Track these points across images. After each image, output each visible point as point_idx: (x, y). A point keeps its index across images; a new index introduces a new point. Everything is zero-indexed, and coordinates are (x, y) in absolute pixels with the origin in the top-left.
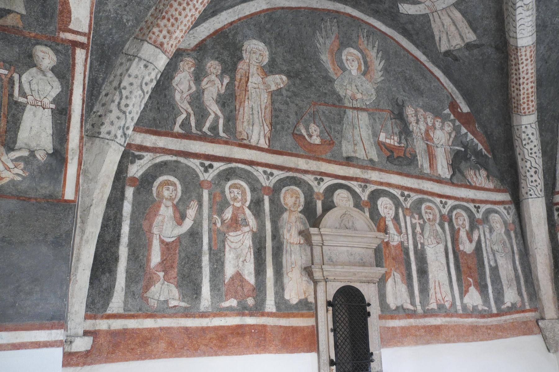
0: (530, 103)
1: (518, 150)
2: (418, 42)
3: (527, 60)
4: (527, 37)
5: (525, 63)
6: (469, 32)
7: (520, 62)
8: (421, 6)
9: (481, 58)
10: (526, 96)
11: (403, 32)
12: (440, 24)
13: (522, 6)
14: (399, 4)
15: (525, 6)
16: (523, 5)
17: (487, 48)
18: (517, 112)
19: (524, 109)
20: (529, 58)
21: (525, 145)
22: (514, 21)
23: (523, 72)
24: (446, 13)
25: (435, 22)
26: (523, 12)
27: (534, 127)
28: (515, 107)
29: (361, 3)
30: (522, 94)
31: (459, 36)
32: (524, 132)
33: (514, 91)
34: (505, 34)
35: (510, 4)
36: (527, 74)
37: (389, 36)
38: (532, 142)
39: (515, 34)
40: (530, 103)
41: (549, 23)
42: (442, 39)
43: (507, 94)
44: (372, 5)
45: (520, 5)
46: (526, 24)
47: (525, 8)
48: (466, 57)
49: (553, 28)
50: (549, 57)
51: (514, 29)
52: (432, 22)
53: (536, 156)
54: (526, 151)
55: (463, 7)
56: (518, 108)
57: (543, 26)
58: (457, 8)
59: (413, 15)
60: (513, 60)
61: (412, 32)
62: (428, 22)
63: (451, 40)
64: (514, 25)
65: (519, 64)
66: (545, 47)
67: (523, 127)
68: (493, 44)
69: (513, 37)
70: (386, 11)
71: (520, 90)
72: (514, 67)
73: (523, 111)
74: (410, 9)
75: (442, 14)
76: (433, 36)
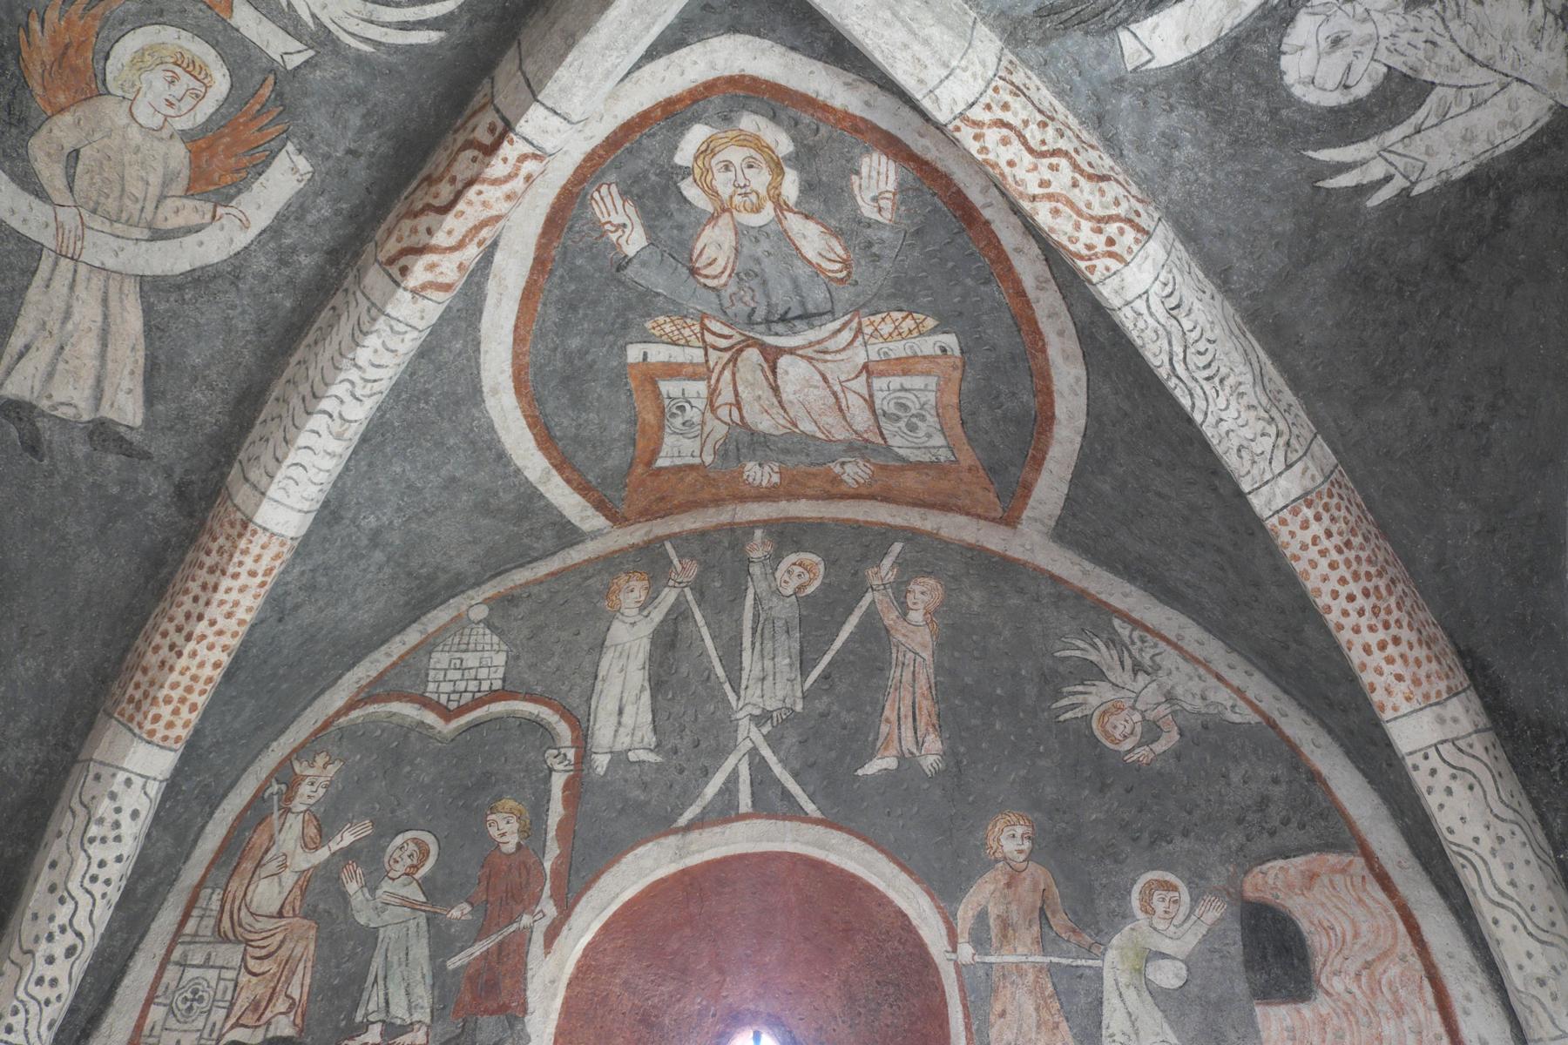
0: (185, 709)
1: (56, 849)
3: (253, 574)
4: (292, 508)
5: (244, 579)
6: (130, 391)
7: (231, 570)
8: (41, 211)
9: (115, 490)
10: (185, 681)
12: (59, 304)
13: (331, 416)
15: (338, 421)
16: (335, 415)
17: (154, 474)
18: (131, 719)
19: (156, 718)
20: (260, 572)
21: (92, 840)
23: (222, 603)
24: (101, 284)
25: (48, 286)
27: (152, 793)
28: (131, 700)
30: (178, 668)
31: (91, 381)
32: (113, 796)
33: (157, 649)
34: (230, 464)
35: (305, 389)
36: (229, 615)
38: (118, 839)
39: (265, 479)
40: (185, 709)
41: (350, 515)
42: (32, 353)
43: (126, 650)
45: (330, 410)
46: (312, 471)
47: (336, 426)
48: (71, 459)
49: (350, 535)
50: (297, 607)
51: (271, 464)
52: (38, 280)
53: (104, 895)
54: (82, 862)
55: (162, 307)
56: (138, 708)
57: (332, 513)
58: (143, 295)
60: (214, 553)
62: (23, 272)
63: (57, 376)
64: (279, 454)
65: (224, 573)
66: (303, 573)
67: (121, 776)
69: (255, 487)
71: (180, 654)
72: (202, 575)
73: (148, 726)
75: (89, 280)
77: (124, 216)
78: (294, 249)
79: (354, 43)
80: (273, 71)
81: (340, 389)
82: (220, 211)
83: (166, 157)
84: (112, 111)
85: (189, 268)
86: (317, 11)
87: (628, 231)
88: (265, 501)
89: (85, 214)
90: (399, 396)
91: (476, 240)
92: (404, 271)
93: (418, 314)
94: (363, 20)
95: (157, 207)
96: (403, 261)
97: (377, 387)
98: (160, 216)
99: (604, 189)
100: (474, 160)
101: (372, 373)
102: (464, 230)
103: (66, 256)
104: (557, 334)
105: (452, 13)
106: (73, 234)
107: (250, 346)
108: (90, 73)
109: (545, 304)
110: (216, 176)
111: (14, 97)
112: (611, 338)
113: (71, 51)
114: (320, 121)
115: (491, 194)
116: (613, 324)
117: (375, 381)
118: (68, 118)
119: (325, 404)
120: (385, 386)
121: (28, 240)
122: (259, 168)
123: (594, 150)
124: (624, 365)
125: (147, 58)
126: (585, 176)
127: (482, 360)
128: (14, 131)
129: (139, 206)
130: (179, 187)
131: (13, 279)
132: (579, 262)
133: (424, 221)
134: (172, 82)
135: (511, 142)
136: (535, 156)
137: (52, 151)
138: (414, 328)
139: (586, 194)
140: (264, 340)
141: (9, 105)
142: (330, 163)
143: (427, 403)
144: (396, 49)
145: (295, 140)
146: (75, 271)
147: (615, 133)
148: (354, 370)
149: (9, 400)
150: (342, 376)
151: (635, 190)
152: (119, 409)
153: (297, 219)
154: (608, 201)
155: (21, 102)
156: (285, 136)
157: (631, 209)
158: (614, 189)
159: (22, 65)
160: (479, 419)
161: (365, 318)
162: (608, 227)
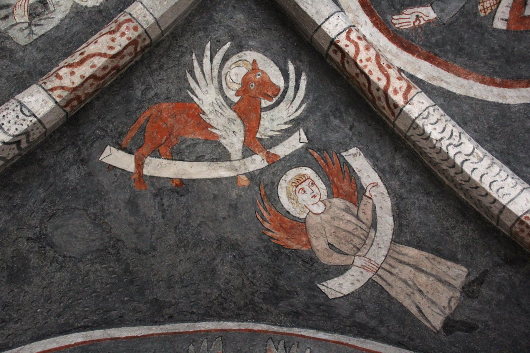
2: (392, 336)
4: (519, 194)
8: (353, 271)
9: (502, 297)
11: (358, 332)
12: (399, 283)
13: (466, 160)
14: (319, 285)
15: (471, 157)
16: (467, 158)
22: (477, 188)
25: (389, 285)
26: (475, 166)
29: (262, 309)
31: (440, 285)
37: (334, 342)
42: (421, 307)
44: (281, 305)
46: (497, 178)
47: (473, 159)
52: (387, 288)
59: (353, 293)
61: (373, 323)
64: (484, 194)
68: (497, 259)
69: (501, 212)
70: (309, 307)
74: (340, 285)
76: (406, 312)
77: (363, 237)
78: (392, 166)
79: (300, 111)
80: (307, 149)
81: (452, 152)
82: (367, 194)
83: (339, 208)
84: (312, 221)
85: (392, 218)
86: (283, 122)
87: (420, 15)
88: (508, 206)
89: (360, 253)
90: (486, 141)
91: (386, 68)
92: (396, 106)
93: (420, 104)
94: (291, 104)
95: (361, 221)
96: (392, 107)
97: (456, 133)
98: (365, 221)
99: (393, 21)
100: (348, 62)
101: (447, 134)
102: (380, 73)
103: (377, 271)
104: (476, 61)
105: (295, 68)
106: (367, 263)
107: (435, 201)
108: (294, 222)
109: (456, 62)
110: (351, 190)
111: (300, 257)
112: (486, 34)
113: (284, 225)
114: (334, 137)
115: (363, 56)
116: (477, 32)
117: (452, 133)
118: (314, 241)
119: (458, 160)
120: (457, 130)
121: (367, 284)
122: (351, 171)
123: (372, 22)
124: (507, 31)
125: (292, 197)
126: (385, 28)
127: (480, 98)
128: (315, 265)
129: (359, 229)
130: (354, 209)
131: (384, 298)
132: (433, 40)
133: (374, 92)
134: (305, 192)
135: (339, 41)
136: (349, 33)
137: (327, 254)
138: (427, 108)
139: (396, 31)
140: (433, 193)
141: (304, 261)
142: (355, 139)
143: (497, 130)
144: (306, 96)
145: (341, 151)
146: (385, 269)
147: (365, 11)
148: (442, 142)
149: (442, 327)
150: (444, 148)
151: (398, 7)
152: (457, 276)
153: (377, 161)
154: (401, 21)
155: (302, 255)
156: (338, 153)
157: (409, 11)
158: (395, 17)
159: (286, 247)
160: (521, 109)
161: (417, 131)
162: (416, 24)
